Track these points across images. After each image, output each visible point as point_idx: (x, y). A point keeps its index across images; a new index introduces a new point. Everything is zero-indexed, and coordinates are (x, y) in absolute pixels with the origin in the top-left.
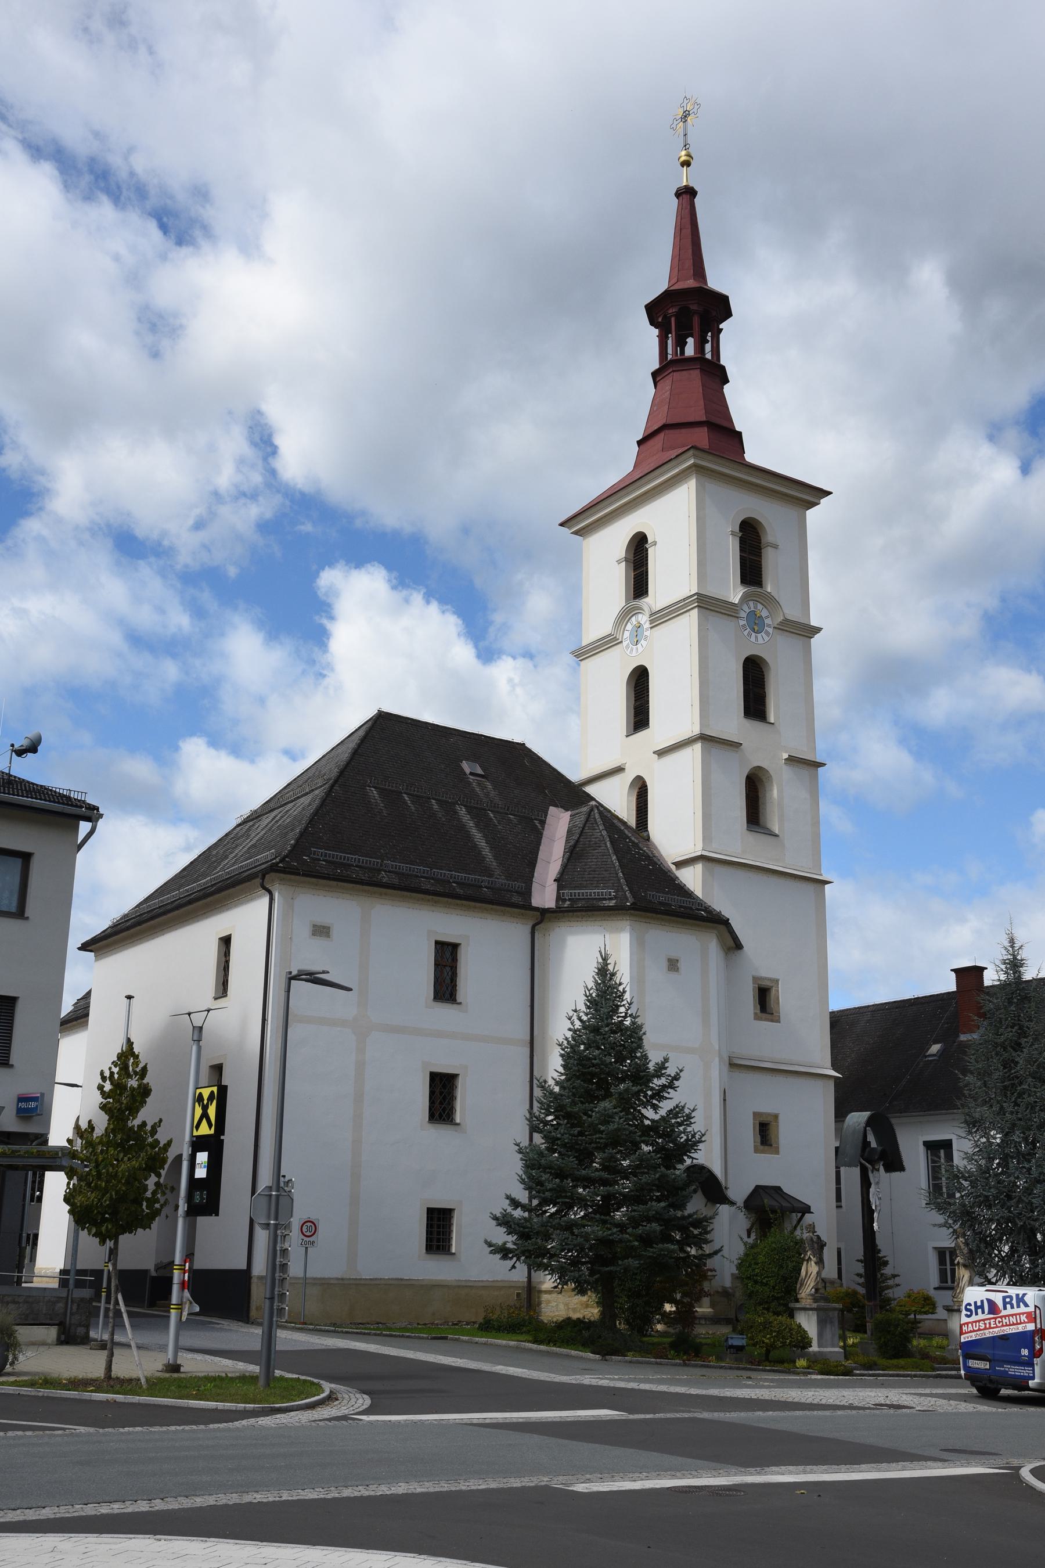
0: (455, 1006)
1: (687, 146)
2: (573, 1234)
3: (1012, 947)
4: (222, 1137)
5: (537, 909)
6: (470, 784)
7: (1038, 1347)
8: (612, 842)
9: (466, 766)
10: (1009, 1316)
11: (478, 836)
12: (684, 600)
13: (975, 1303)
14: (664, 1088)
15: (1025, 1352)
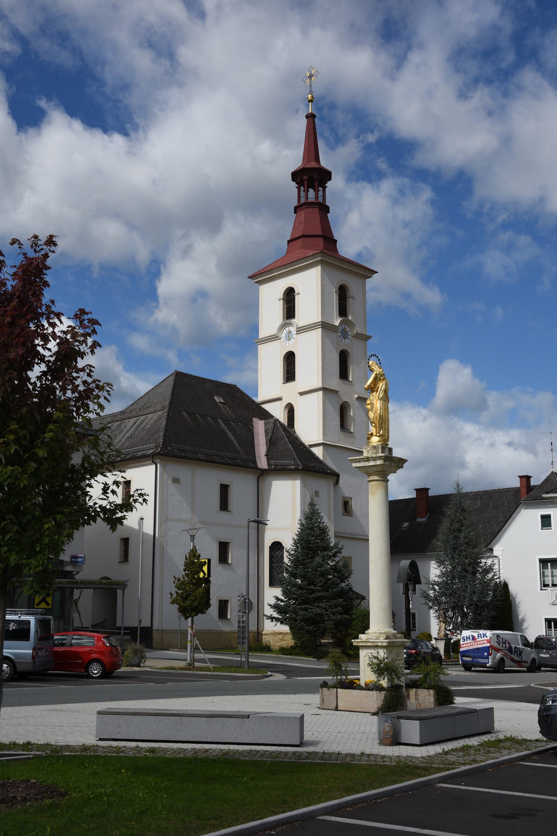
0: (228, 512)
1: (312, 92)
2: (307, 611)
3: (458, 488)
4: (210, 579)
5: (260, 469)
6: (220, 407)
7: (491, 652)
8: (287, 438)
9: (217, 399)
10: (480, 641)
11: (230, 434)
12: (315, 323)
13: (467, 636)
14: (336, 552)
15: (486, 654)
